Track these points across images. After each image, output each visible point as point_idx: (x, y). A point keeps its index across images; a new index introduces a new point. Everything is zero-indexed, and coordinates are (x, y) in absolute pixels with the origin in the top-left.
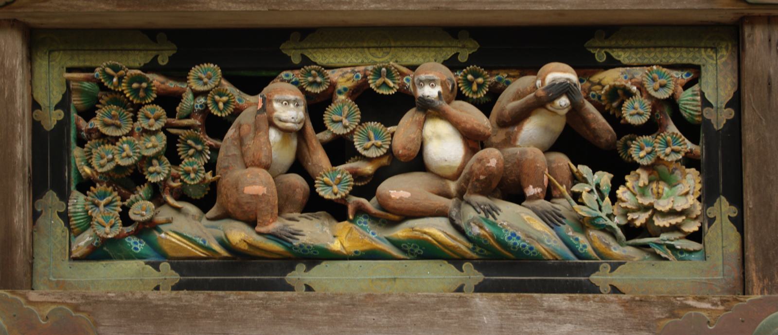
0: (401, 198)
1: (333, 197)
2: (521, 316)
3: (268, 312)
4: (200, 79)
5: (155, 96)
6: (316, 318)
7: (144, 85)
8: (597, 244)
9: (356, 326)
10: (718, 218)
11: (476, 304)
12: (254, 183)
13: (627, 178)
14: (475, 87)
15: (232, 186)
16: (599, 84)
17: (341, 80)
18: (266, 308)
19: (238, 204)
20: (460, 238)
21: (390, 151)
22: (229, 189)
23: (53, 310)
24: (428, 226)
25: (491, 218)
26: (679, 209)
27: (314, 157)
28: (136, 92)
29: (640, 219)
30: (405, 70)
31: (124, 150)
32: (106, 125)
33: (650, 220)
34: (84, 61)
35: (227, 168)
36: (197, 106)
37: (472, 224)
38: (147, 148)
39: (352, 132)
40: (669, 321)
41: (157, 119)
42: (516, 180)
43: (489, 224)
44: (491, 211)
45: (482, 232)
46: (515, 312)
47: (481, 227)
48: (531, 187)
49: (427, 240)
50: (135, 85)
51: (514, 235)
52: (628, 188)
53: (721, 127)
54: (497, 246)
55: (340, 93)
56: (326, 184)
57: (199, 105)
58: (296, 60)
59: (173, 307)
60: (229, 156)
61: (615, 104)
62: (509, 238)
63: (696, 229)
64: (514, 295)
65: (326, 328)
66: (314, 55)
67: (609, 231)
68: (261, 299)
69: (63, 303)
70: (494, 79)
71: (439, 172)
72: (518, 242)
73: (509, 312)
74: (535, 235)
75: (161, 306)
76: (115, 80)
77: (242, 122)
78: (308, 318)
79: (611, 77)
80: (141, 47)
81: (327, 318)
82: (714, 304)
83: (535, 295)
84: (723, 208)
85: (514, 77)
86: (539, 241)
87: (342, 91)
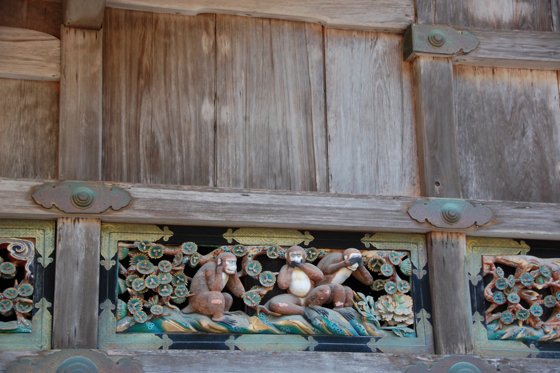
0: (284, 307)
1: (253, 306)
2: (344, 363)
3: (226, 360)
4: (186, 249)
5: (162, 255)
6: (249, 363)
7: (159, 251)
8: (369, 329)
9: (268, 367)
11: (323, 357)
12: (217, 299)
13: (379, 299)
14: (311, 257)
15: (204, 299)
16: (365, 257)
17: (252, 251)
18: (225, 358)
19: (207, 308)
20: (309, 325)
21: (276, 284)
22: (201, 301)
23: (121, 359)
24: (295, 319)
25: (326, 317)
26: (406, 314)
27: (238, 286)
28: (153, 253)
29: (388, 318)
30: (280, 248)
31: (150, 281)
32: (141, 269)
33: (393, 319)
34: (127, 238)
35: (200, 290)
37: (317, 319)
38: (162, 280)
39: (258, 276)
40: (410, 366)
41: (167, 267)
42: (331, 298)
44: (325, 313)
45: (321, 323)
46: (341, 361)
47: (321, 321)
48: (339, 302)
49: (294, 326)
50: (155, 251)
51: (335, 324)
52: (382, 304)
53: (421, 278)
54: (326, 329)
55: (250, 256)
56: (248, 299)
58: (230, 241)
59: (180, 357)
61: (374, 266)
62: (333, 326)
63: (413, 323)
64: (340, 353)
65: (254, 368)
67: (374, 323)
68: (223, 354)
69: (125, 356)
70: (319, 253)
71: (298, 295)
73: (338, 361)
74: (342, 324)
75: (174, 357)
76: (145, 248)
77: (208, 269)
78: (246, 363)
79: (371, 254)
80: (157, 232)
82: (429, 359)
83: (350, 353)
84: (424, 314)
85: (327, 252)
86: (345, 327)
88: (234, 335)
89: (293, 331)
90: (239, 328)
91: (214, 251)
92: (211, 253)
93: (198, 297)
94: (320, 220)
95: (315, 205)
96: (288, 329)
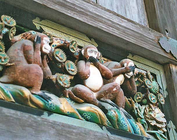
10: (171, 128)
18: (53, 128)
36: (3, 32)
43: (118, 112)
49: (96, 113)
57: (4, 31)
60: (19, 56)
66: (45, 28)
72: (124, 122)
75: (9, 116)
81: (76, 137)
87: (55, 46)
88: (47, 112)
89: (92, 119)
90: (54, 105)
91: (23, 34)
92: (20, 35)
93: (18, 67)
94: (109, 29)
95: (104, 16)
96: (89, 115)
